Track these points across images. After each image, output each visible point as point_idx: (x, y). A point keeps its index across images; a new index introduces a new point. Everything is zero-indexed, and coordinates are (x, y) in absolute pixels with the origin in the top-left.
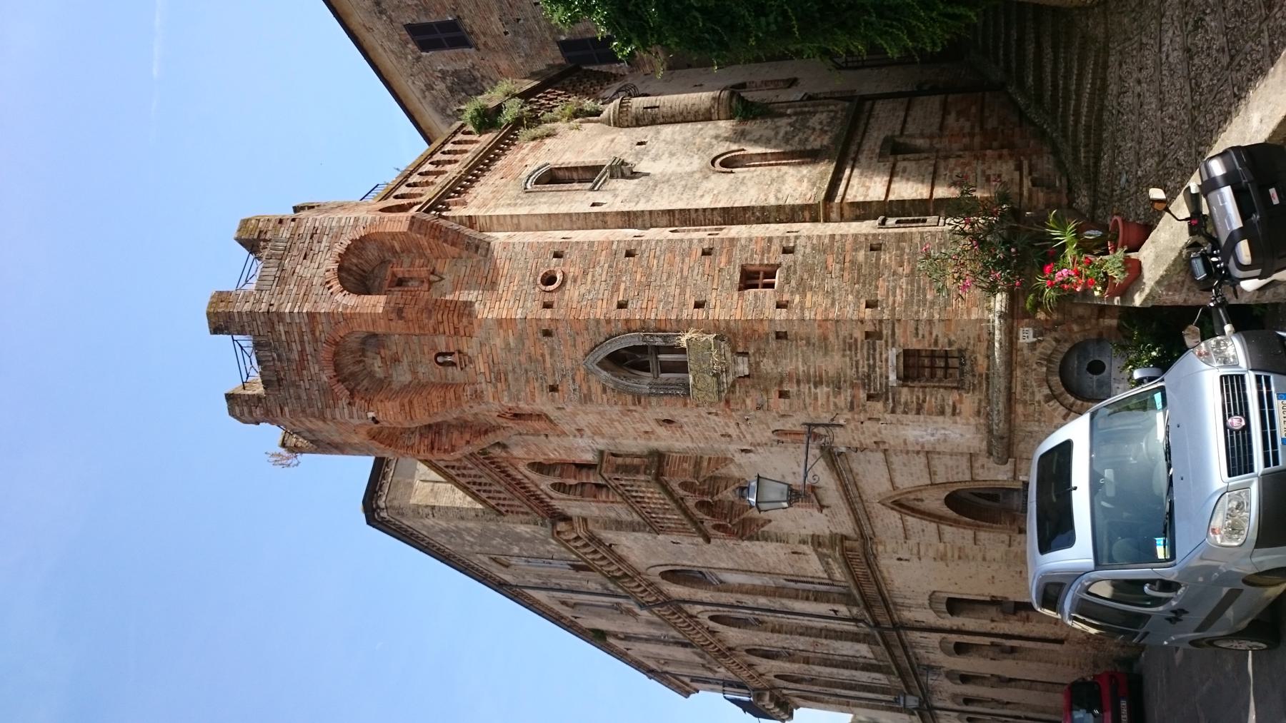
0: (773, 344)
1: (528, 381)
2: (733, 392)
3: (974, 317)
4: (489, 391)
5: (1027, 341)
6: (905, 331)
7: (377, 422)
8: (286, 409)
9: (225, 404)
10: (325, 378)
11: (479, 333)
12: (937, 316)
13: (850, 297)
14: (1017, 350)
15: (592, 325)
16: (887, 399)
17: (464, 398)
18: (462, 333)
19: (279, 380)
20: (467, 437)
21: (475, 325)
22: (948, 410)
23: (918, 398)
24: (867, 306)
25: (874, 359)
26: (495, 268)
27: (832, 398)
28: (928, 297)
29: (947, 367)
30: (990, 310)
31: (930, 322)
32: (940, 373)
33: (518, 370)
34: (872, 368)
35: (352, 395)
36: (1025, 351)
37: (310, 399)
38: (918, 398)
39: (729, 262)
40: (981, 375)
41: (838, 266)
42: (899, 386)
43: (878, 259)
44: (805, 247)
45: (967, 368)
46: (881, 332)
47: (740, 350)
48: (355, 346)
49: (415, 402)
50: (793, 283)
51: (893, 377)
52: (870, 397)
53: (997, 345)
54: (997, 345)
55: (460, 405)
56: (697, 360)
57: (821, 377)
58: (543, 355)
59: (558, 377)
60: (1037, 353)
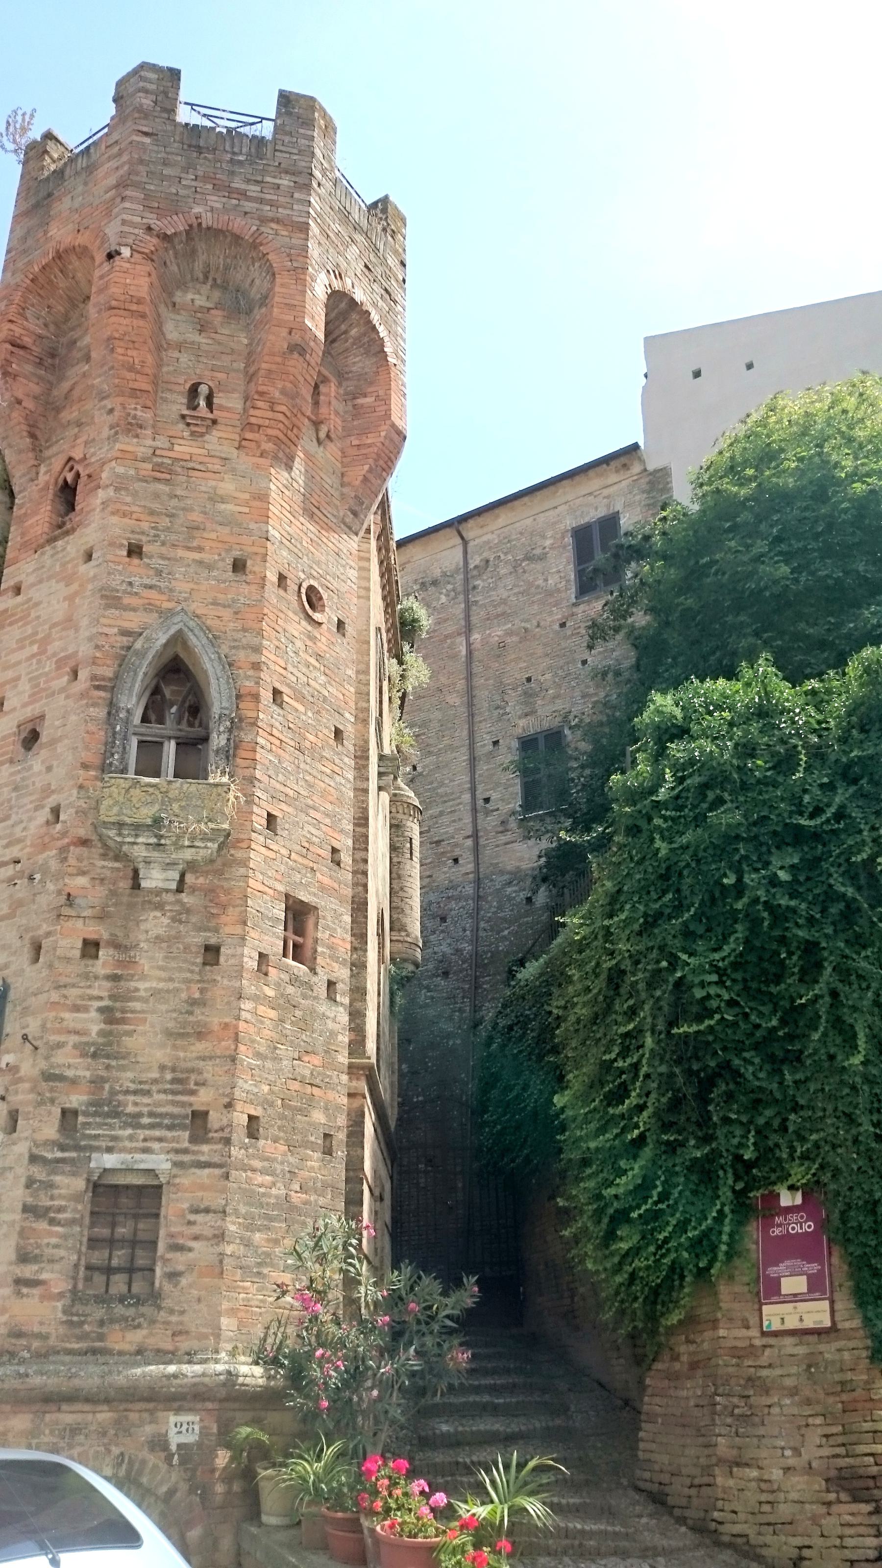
0: (198, 939)
1: (152, 513)
2: (104, 856)
3: (225, 1322)
4: (141, 446)
5: (172, 1432)
6: (202, 1187)
7: (110, 256)
8: (147, 140)
9: (165, 61)
10: (197, 210)
11: (244, 462)
12: (229, 1249)
13: (266, 1088)
14: (152, 1412)
15: (249, 639)
16: (62, 1148)
17: (131, 404)
18: (249, 435)
19: (199, 149)
20: (29, 404)
21: (261, 461)
22: (28, 1271)
23: (60, 1210)
24: (250, 1117)
25: (152, 1126)
26: (330, 529)
27: (73, 1039)
28: (258, 1235)
29: (109, 1271)
30: (233, 1353)
31: (220, 1237)
32: (98, 1257)
33: (174, 502)
34: (134, 1121)
35: (165, 238)
36: (149, 1429)
37: (163, 178)
38: (60, 1210)
39: (323, 888)
40: (101, 1337)
41: (307, 1073)
42: (90, 1172)
43: (313, 1147)
44: (334, 1020)
45: (119, 1310)
46: (207, 1141)
47: (189, 878)
48: (237, 276)
49: (141, 323)
50: (290, 990)
51: (110, 1161)
52: (68, 1115)
53: (172, 1369)
54: (172, 1369)
55: (122, 394)
56: (188, 797)
57: (123, 1021)
58: (200, 549)
59: (156, 562)
60: (145, 1454)
